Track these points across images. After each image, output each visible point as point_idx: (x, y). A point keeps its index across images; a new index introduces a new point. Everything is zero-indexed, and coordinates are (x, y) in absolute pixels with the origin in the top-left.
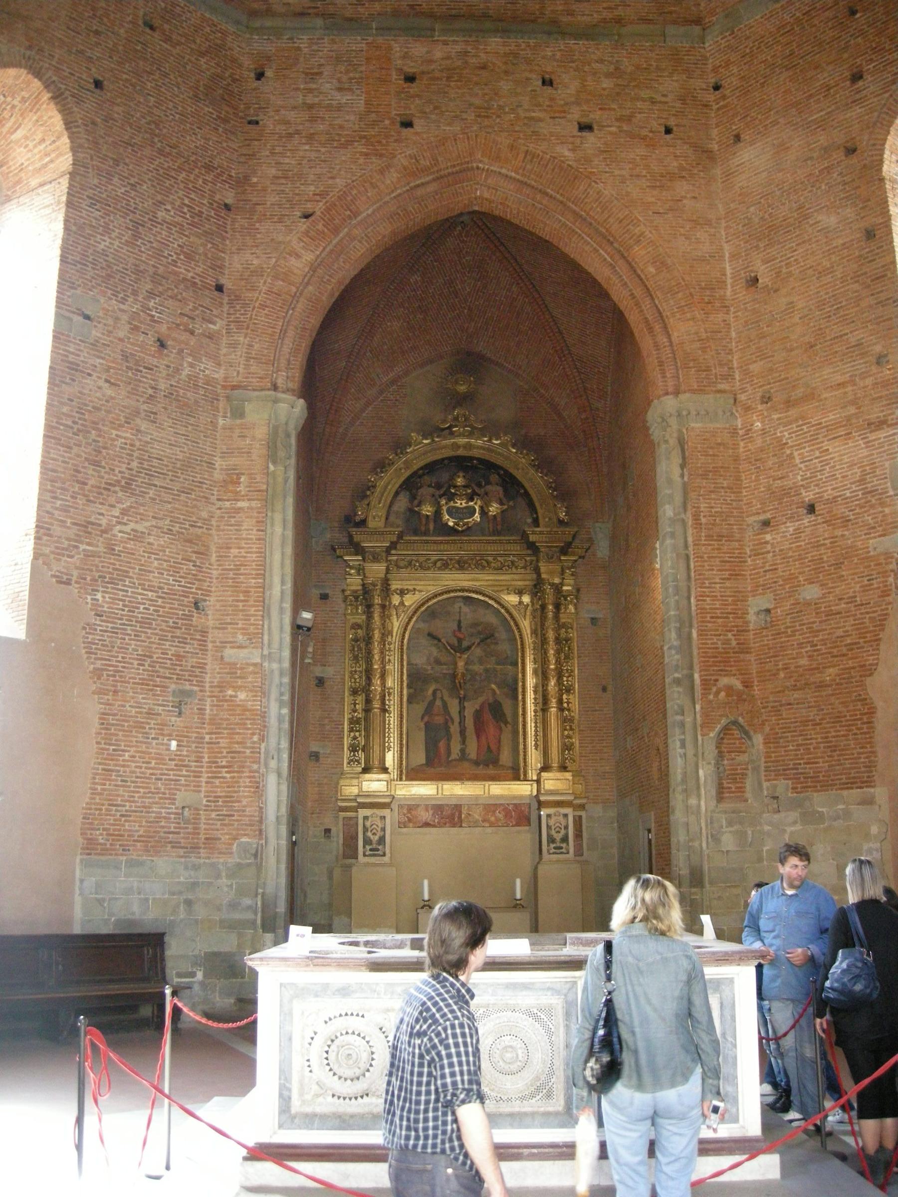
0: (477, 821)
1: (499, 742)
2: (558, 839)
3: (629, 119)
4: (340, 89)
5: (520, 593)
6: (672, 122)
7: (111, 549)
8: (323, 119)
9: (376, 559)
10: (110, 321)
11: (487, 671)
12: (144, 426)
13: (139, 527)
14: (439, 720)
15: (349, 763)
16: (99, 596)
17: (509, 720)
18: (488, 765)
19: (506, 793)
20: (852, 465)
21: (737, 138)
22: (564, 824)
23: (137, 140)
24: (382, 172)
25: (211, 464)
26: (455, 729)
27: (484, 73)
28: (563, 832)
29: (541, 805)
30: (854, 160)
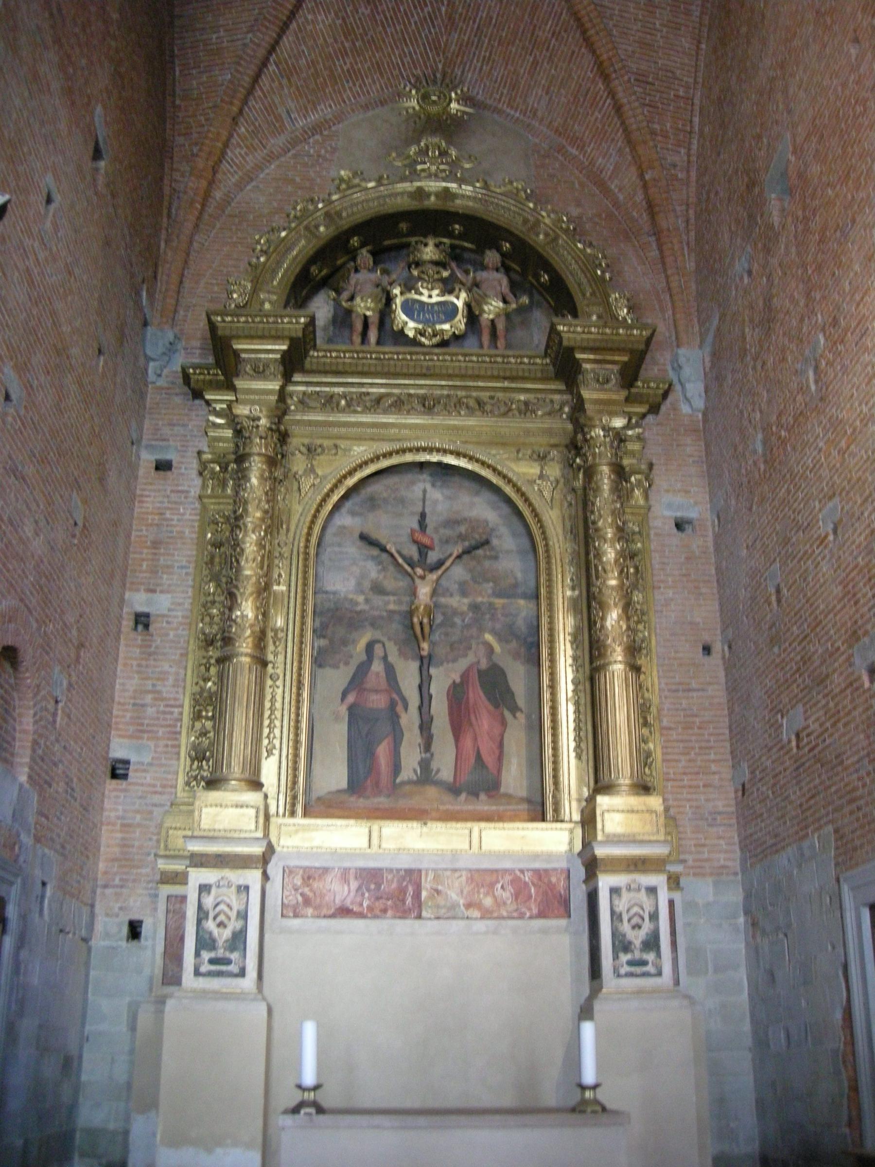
0: (454, 906)
1: (501, 745)
2: (637, 943)
9: (260, 371)
11: (475, 607)
14: (378, 701)
15: (188, 784)
17: (521, 702)
18: (477, 795)
19: (516, 847)
22: (648, 907)
26: (410, 719)
28: (647, 926)
29: (592, 866)
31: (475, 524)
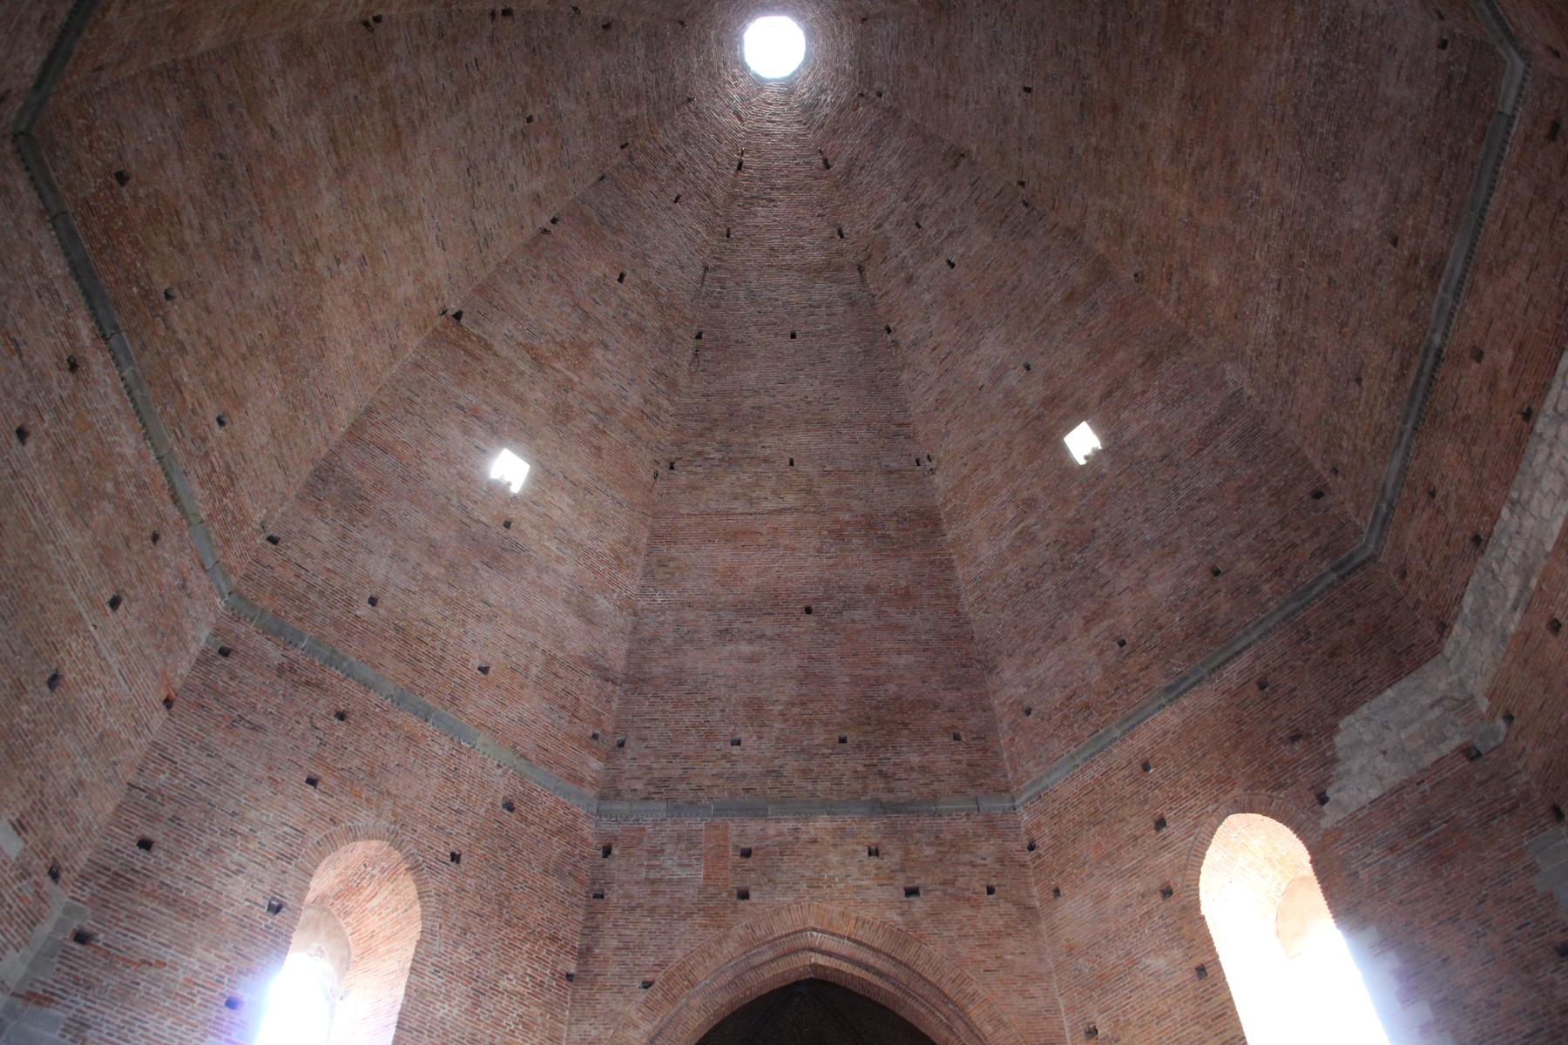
3: (952, 882)
4: (680, 865)
6: (993, 882)
8: (664, 893)
21: (1057, 892)
23: (486, 910)
24: (719, 942)
27: (815, 848)
30: (1172, 902)
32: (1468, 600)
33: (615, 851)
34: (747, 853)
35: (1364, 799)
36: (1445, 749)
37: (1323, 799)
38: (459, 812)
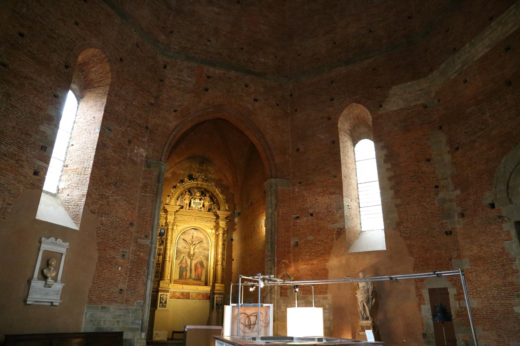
4: (188, 76)
5: (212, 229)
6: (279, 103)
7: (108, 204)
9: (171, 215)
10: (116, 133)
11: (199, 252)
12: (122, 166)
13: (118, 198)
14: (184, 266)
16: (103, 218)
20: (324, 204)
21: (296, 110)
25: (139, 181)
26: (188, 269)
31: (201, 238)
32: (443, 65)
33: (168, 68)
34: (209, 77)
35: (392, 109)
36: (419, 103)
37: (381, 106)
38: (123, 44)
